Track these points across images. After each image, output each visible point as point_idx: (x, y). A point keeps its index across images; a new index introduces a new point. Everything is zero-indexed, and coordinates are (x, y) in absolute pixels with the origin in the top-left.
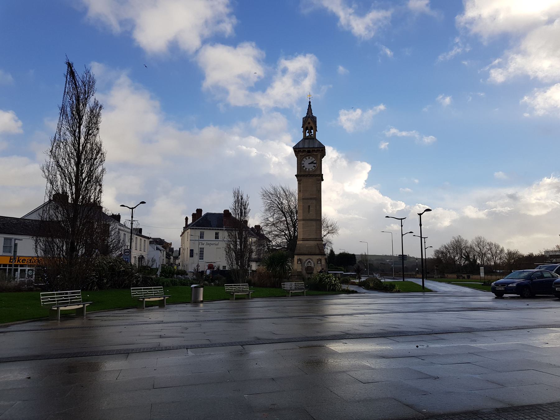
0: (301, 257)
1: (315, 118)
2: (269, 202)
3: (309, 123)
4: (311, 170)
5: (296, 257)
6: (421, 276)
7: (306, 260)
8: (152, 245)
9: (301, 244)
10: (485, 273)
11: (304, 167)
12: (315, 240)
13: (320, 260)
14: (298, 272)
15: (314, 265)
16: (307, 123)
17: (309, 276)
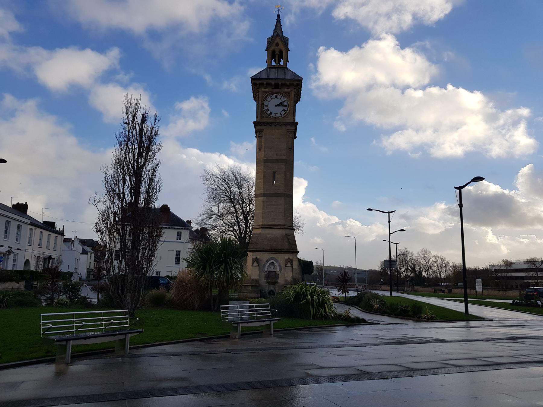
1: (287, 39)
2: (214, 187)
3: (277, 45)
4: (278, 115)
5: (250, 256)
6: (389, 288)
7: (267, 261)
8: (67, 243)
9: (259, 234)
10: (484, 286)
12: (283, 227)
13: (291, 261)
14: (253, 280)
15: (281, 269)
16: (274, 44)
17: (272, 287)
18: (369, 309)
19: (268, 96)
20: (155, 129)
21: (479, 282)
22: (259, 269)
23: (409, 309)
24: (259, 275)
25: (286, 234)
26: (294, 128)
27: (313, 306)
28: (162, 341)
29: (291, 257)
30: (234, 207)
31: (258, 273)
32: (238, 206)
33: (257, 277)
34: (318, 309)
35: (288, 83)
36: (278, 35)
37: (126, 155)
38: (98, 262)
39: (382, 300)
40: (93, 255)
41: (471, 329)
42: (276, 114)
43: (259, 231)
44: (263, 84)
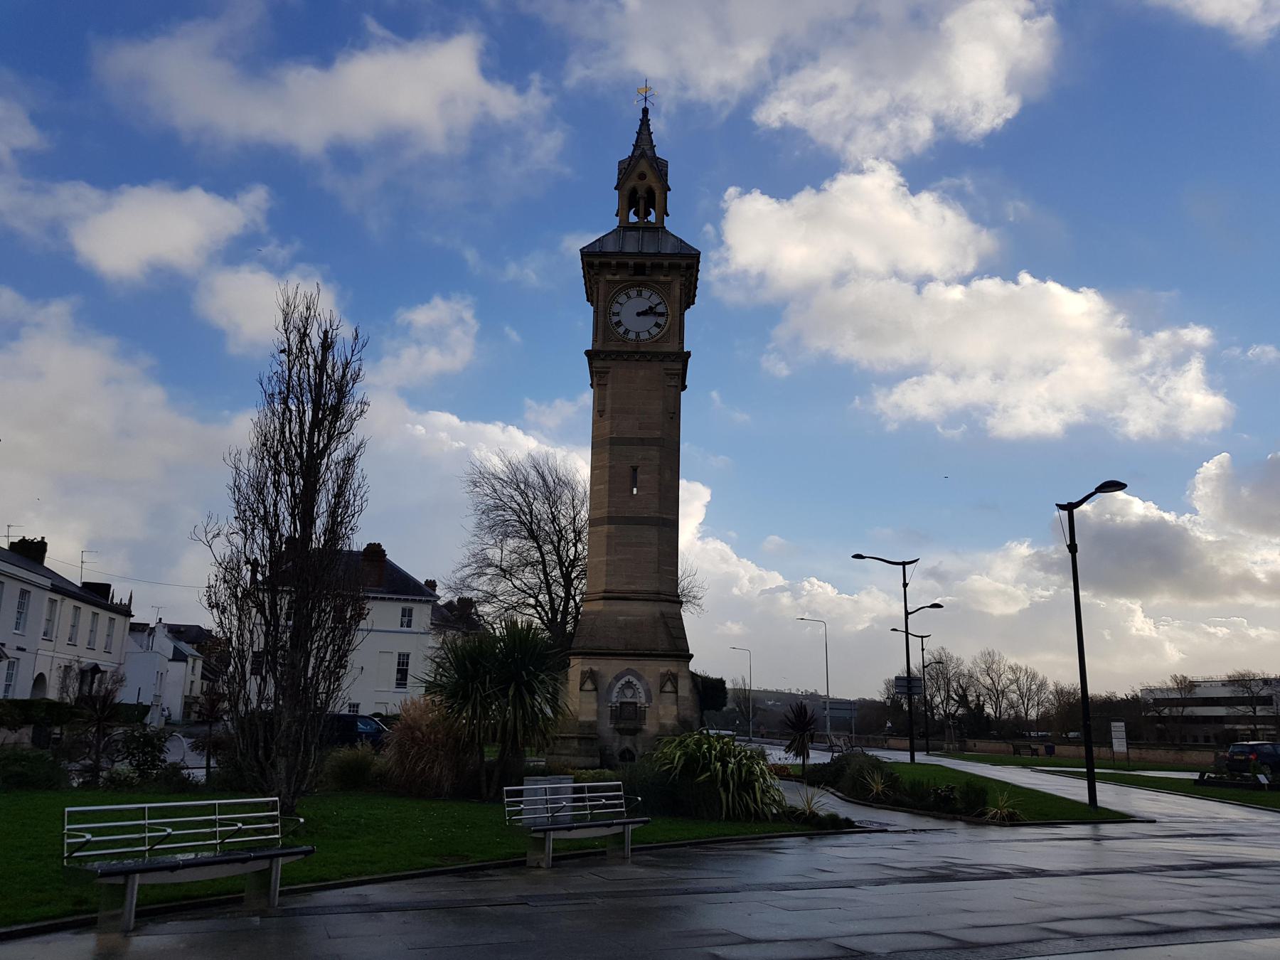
0: (597, 665)
1: (664, 164)
2: (491, 502)
3: (642, 176)
5: (577, 667)
6: (907, 743)
7: (617, 678)
8: (138, 635)
9: (598, 613)
10: (1133, 738)
12: (656, 597)
13: (673, 678)
14: (582, 725)
15: (649, 699)
17: (627, 743)
18: (859, 794)
19: (619, 292)
20: (355, 366)
21: (1118, 728)
22: (598, 700)
23: (957, 795)
24: (598, 713)
25: (662, 614)
26: (680, 366)
27: (727, 789)
28: (360, 874)
29: (674, 670)
30: (540, 548)
31: (595, 706)
32: (548, 547)
33: (594, 718)
34: (739, 795)
35: (666, 263)
36: (643, 155)
37: (282, 425)
38: (210, 680)
39: (889, 772)
40: (199, 663)
41: (1106, 843)
42: (638, 334)
43: (598, 606)
44: (609, 265)
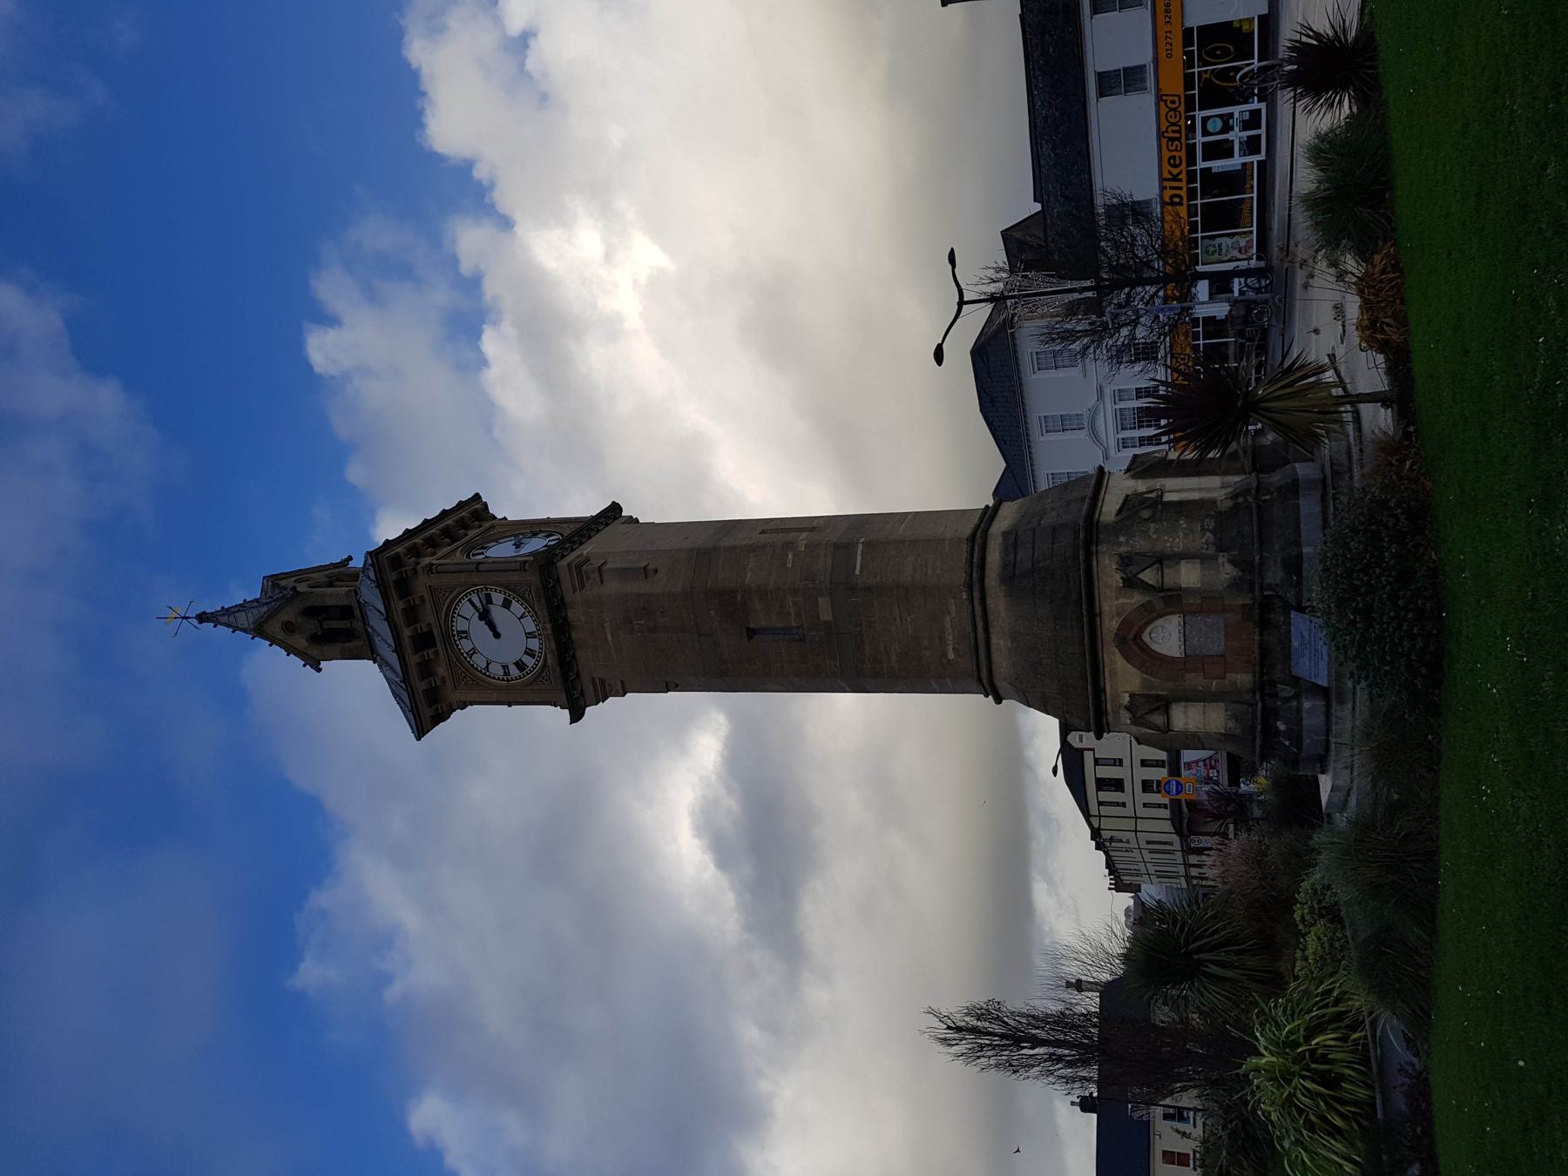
11: (520, 665)
42: (529, 635)
